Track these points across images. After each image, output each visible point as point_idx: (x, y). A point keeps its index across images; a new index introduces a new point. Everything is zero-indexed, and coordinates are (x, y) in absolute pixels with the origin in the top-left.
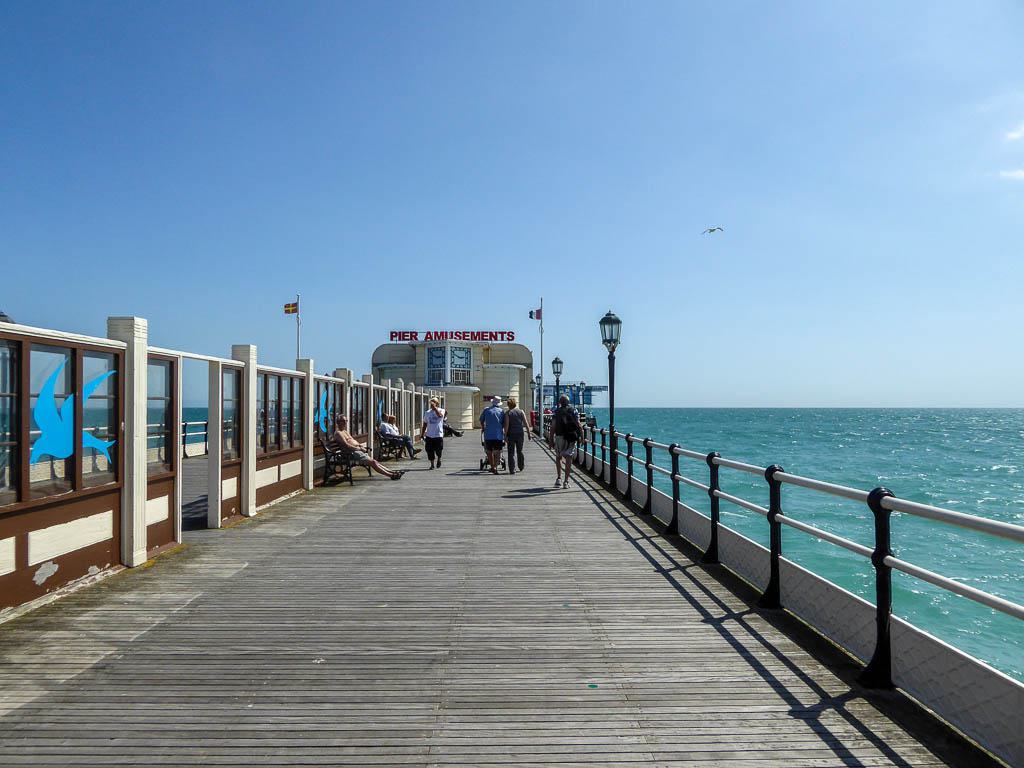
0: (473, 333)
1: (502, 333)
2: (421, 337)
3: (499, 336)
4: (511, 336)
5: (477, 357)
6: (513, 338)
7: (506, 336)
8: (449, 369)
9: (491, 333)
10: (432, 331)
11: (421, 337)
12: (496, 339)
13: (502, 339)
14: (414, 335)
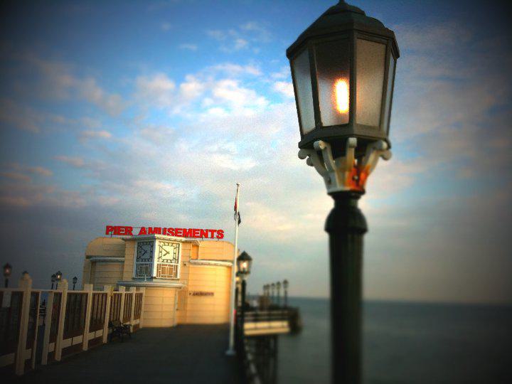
0: (185, 230)
1: (213, 231)
2: (136, 232)
3: (210, 234)
4: (221, 234)
6: (222, 237)
7: (215, 234)
9: (202, 230)
10: (147, 227)
11: (136, 232)
13: (212, 237)
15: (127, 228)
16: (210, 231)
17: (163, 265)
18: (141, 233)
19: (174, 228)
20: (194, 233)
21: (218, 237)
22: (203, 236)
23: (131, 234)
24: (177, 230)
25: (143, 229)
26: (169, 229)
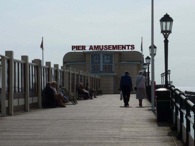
0: (113, 46)
1: (128, 46)
2: (87, 49)
3: (127, 47)
4: (133, 47)
5: (115, 59)
6: (134, 48)
7: (130, 47)
8: (102, 64)
9: (123, 46)
10: (93, 45)
11: (87, 49)
12: (125, 49)
13: (128, 49)
14: (84, 47)
15: (82, 46)
16: (127, 45)
17: (105, 65)
18: (90, 49)
19: (107, 45)
20: (119, 47)
21: (131, 49)
22: (124, 49)
23: (85, 50)
24: (109, 46)
25: (91, 46)
26: (105, 46)
